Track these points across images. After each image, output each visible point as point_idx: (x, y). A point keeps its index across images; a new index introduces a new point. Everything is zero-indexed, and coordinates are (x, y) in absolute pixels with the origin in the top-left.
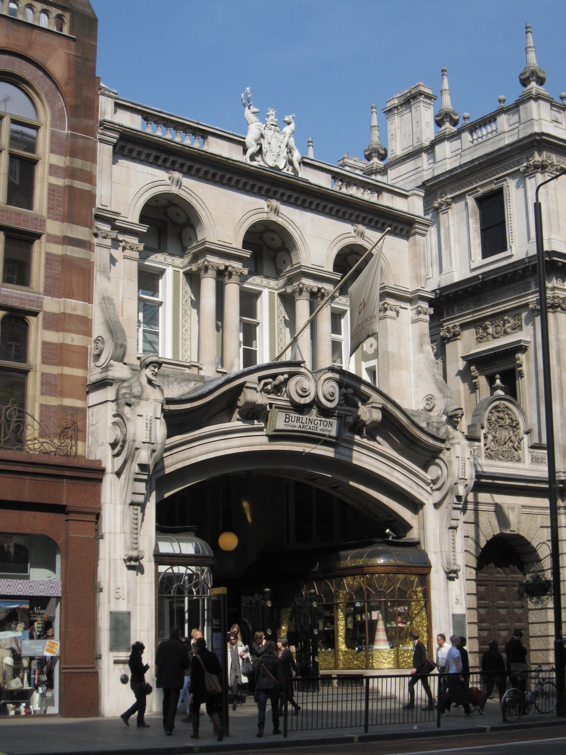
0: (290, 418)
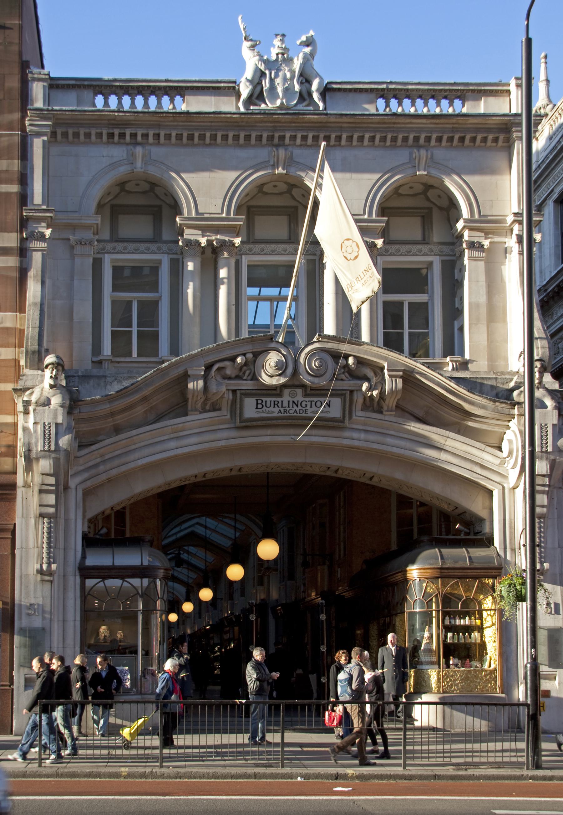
0: (264, 403)
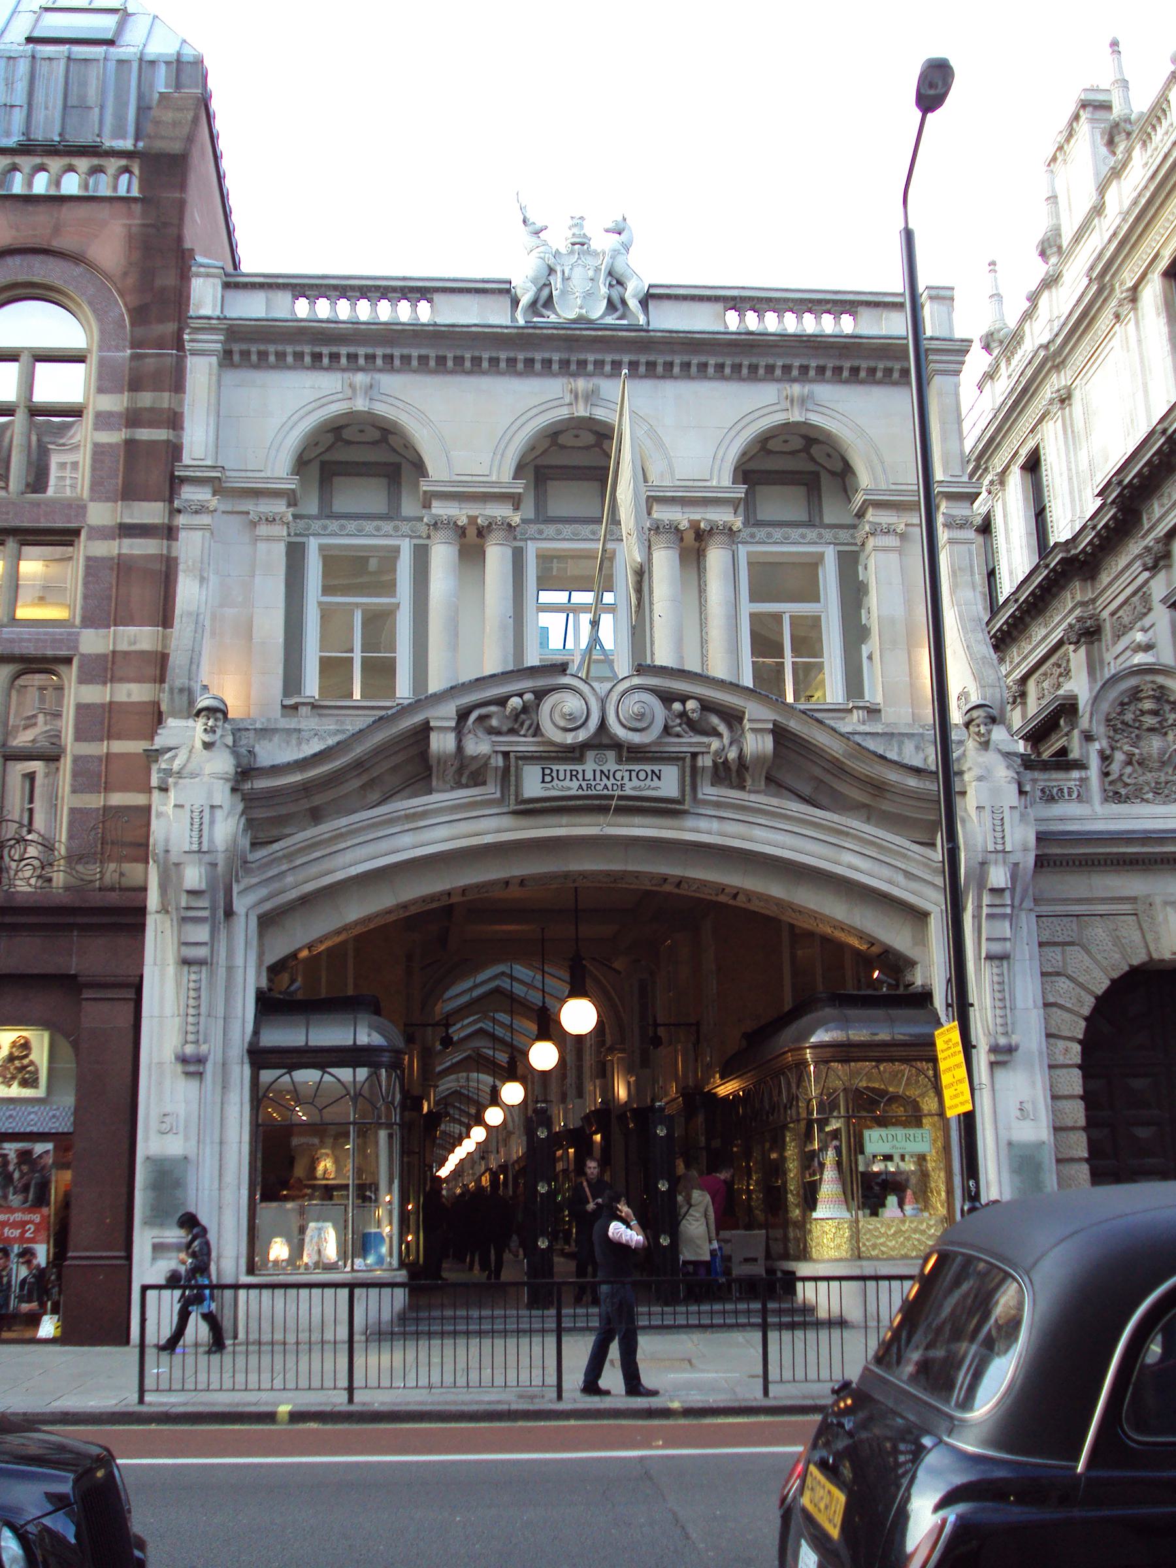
0: (554, 774)
